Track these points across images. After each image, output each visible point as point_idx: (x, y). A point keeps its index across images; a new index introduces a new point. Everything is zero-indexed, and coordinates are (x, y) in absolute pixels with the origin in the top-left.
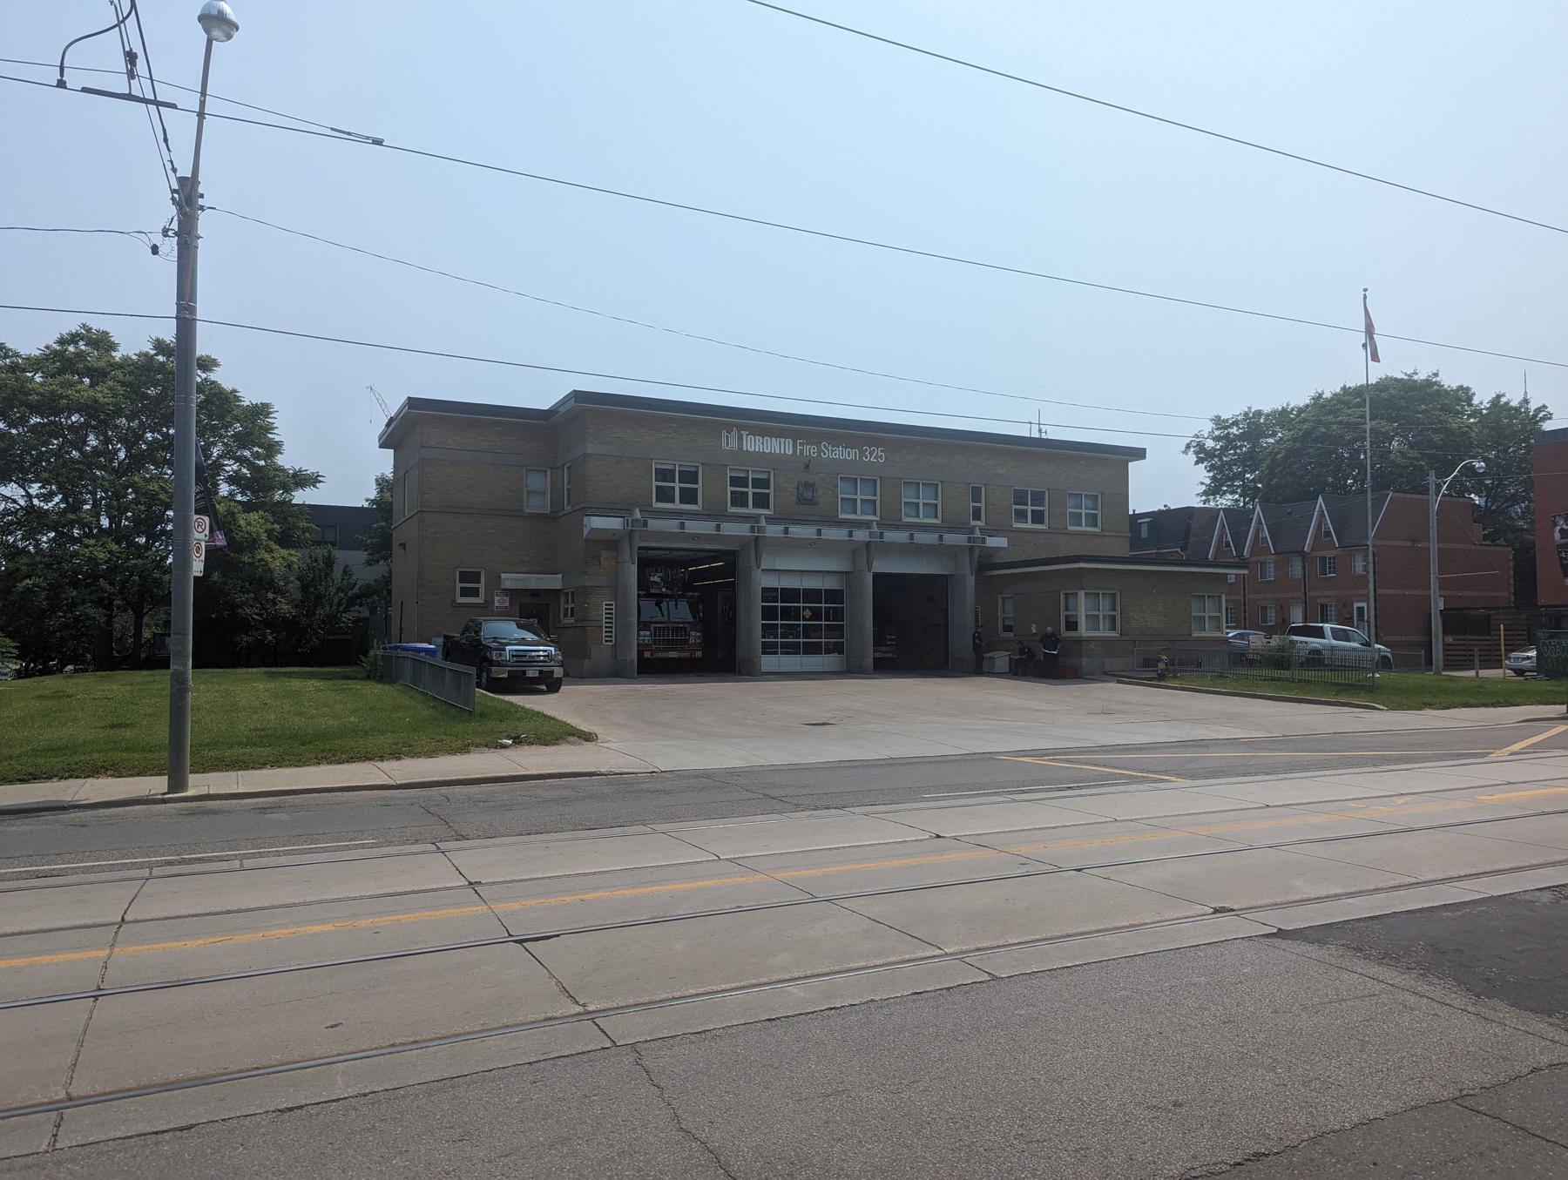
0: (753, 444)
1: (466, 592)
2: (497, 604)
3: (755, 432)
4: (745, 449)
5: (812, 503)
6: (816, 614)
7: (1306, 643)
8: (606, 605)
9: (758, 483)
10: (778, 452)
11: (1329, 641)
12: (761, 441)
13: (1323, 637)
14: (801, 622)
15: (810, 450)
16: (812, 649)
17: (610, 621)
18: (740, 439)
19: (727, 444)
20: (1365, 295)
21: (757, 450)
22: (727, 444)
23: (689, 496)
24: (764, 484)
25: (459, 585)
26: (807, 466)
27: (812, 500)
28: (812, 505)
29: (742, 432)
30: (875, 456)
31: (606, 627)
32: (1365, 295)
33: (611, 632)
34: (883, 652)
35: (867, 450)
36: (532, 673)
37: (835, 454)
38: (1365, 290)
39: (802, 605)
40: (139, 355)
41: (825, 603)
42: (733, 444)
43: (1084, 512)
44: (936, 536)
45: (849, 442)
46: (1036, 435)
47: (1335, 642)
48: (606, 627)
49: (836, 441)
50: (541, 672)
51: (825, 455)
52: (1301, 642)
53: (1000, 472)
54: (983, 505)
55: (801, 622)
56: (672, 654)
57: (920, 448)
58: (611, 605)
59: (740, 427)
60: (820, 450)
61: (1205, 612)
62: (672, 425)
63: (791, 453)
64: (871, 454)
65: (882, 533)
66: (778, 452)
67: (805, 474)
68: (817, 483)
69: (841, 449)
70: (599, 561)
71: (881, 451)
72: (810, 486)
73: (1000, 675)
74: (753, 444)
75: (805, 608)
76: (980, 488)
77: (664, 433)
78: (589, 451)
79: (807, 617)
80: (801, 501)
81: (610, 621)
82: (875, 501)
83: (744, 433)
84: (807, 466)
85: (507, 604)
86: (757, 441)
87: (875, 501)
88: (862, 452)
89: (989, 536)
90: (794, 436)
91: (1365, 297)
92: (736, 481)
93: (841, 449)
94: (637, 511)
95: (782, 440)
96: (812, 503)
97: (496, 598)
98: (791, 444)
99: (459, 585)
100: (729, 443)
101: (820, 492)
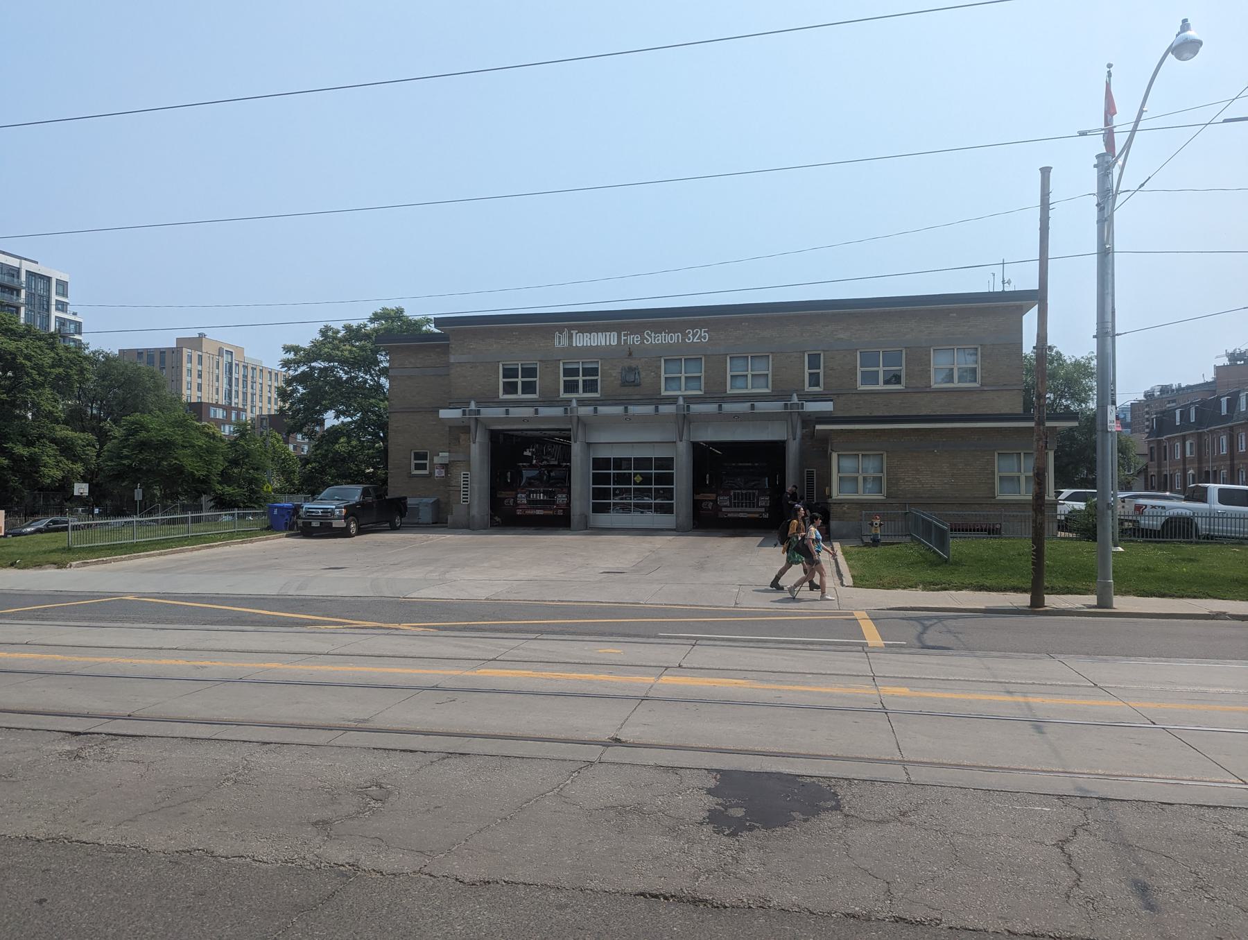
0: (582, 340)
1: (418, 467)
2: (437, 475)
3: (582, 330)
4: (574, 345)
5: (635, 384)
6: (647, 479)
7: (1163, 508)
8: (464, 474)
9: (587, 372)
10: (603, 344)
11: (1215, 505)
12: (589, 337)
13: (1204, 500)
14: (632, 486)
15: (634, 340)
16: (643, 508)
17: (466, 490)
18: (571, 337)
19: (560, 343)
20: (1109, 72)
21: (585, 345)
22: (560, 343)
23: (528, 388)
24: (594, 371)
25: (414, 462)
26: (630, 354)
27: (634, 382)
28: (635, 386)
29: (572, 332)
30: (698, 337)
31: (463, 491)
32: (1109, 72)
33: (467, 495)
34: (748, 513)
35: (689, 332)
36: (315, 524)
37: (658, 340)
38: (1110, 66)
39: (632, 471)
40: (376, 317)
41: (652, 473)
42: (564, 342)
43: (537, 379)
44: (532, 410)
45: (671, 328)
46: (999, 289)
47: (1221, 508)
48: (463, 491)
49: (658, 328)
50: (321, 523)
51: (648, 342)
52: (1153, 507)
53: (842, 336)
54: (821, 371)
55: (632, 486)
56: (539, 512)
57: (747, 324)
58: (468, 474)
59: (570, 328)
60: (643, 338)
61: (1020, 471)
62: (514, 333)
63: (616, 343)
64: (694, 335)
65: (688, 407)
66: (603, 344)
67: (629, 360)
68: (640, 367)
69: (663, 334)
70: (459, 441)
71: (705, 332)
72: (631, 370)
73: (467, 526)
74: (582, 340)
75: (635, 474)
76: (820, 354)
77: (508, 340)
78: (452, 361)
79: (638, 482)
80: (625, 383)
81: (466, 490)
82: (767, 375)
83: (574, 332)
84: (630, 354)
85: (443, 475)
86: (585, 337)
87: (767, 375)
88: (685, 335)
89: (806, 401)
90: (618, 329)
91: (1109, 74)
92: (568, 372)
93: (663, 334)
94: (795, 395)
95: (608, 334)
96: (635, 384)
97: (436, 471)
98: (616, 336)
99: (414, 462)
100: (561, 342)
101: (643, 374)
